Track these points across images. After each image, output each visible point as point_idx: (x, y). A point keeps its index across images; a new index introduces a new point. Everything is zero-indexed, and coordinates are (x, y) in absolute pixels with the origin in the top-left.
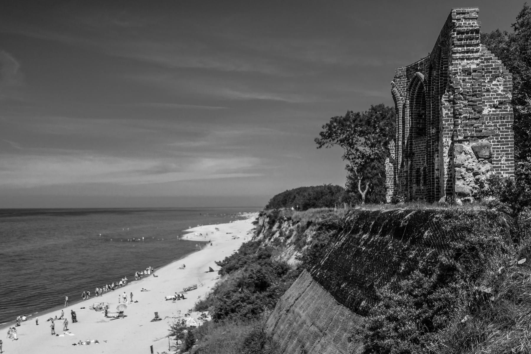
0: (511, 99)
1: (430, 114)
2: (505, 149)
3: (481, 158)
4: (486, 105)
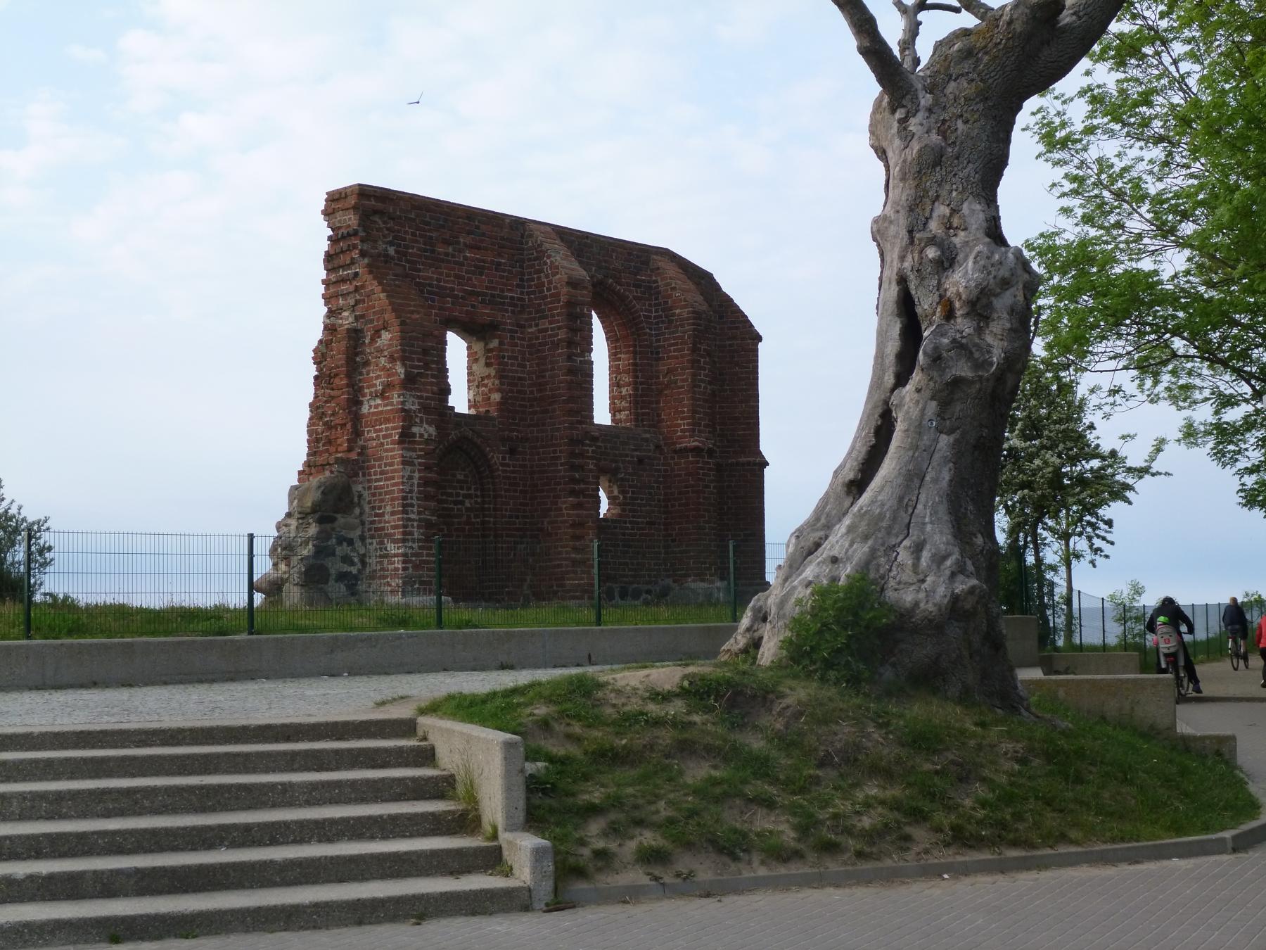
0: (402, 376)
2: (390, 489)
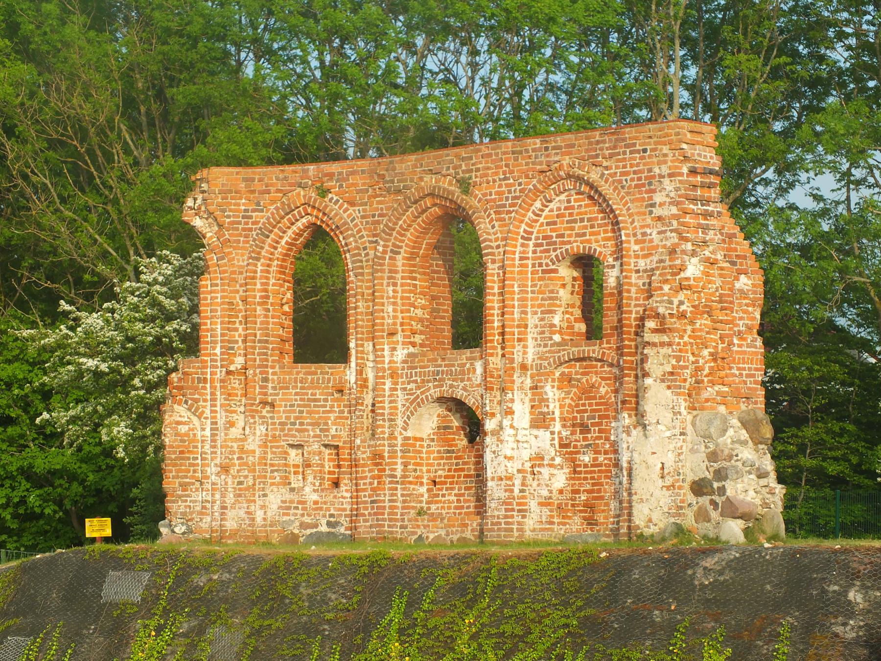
3: (761, 443)
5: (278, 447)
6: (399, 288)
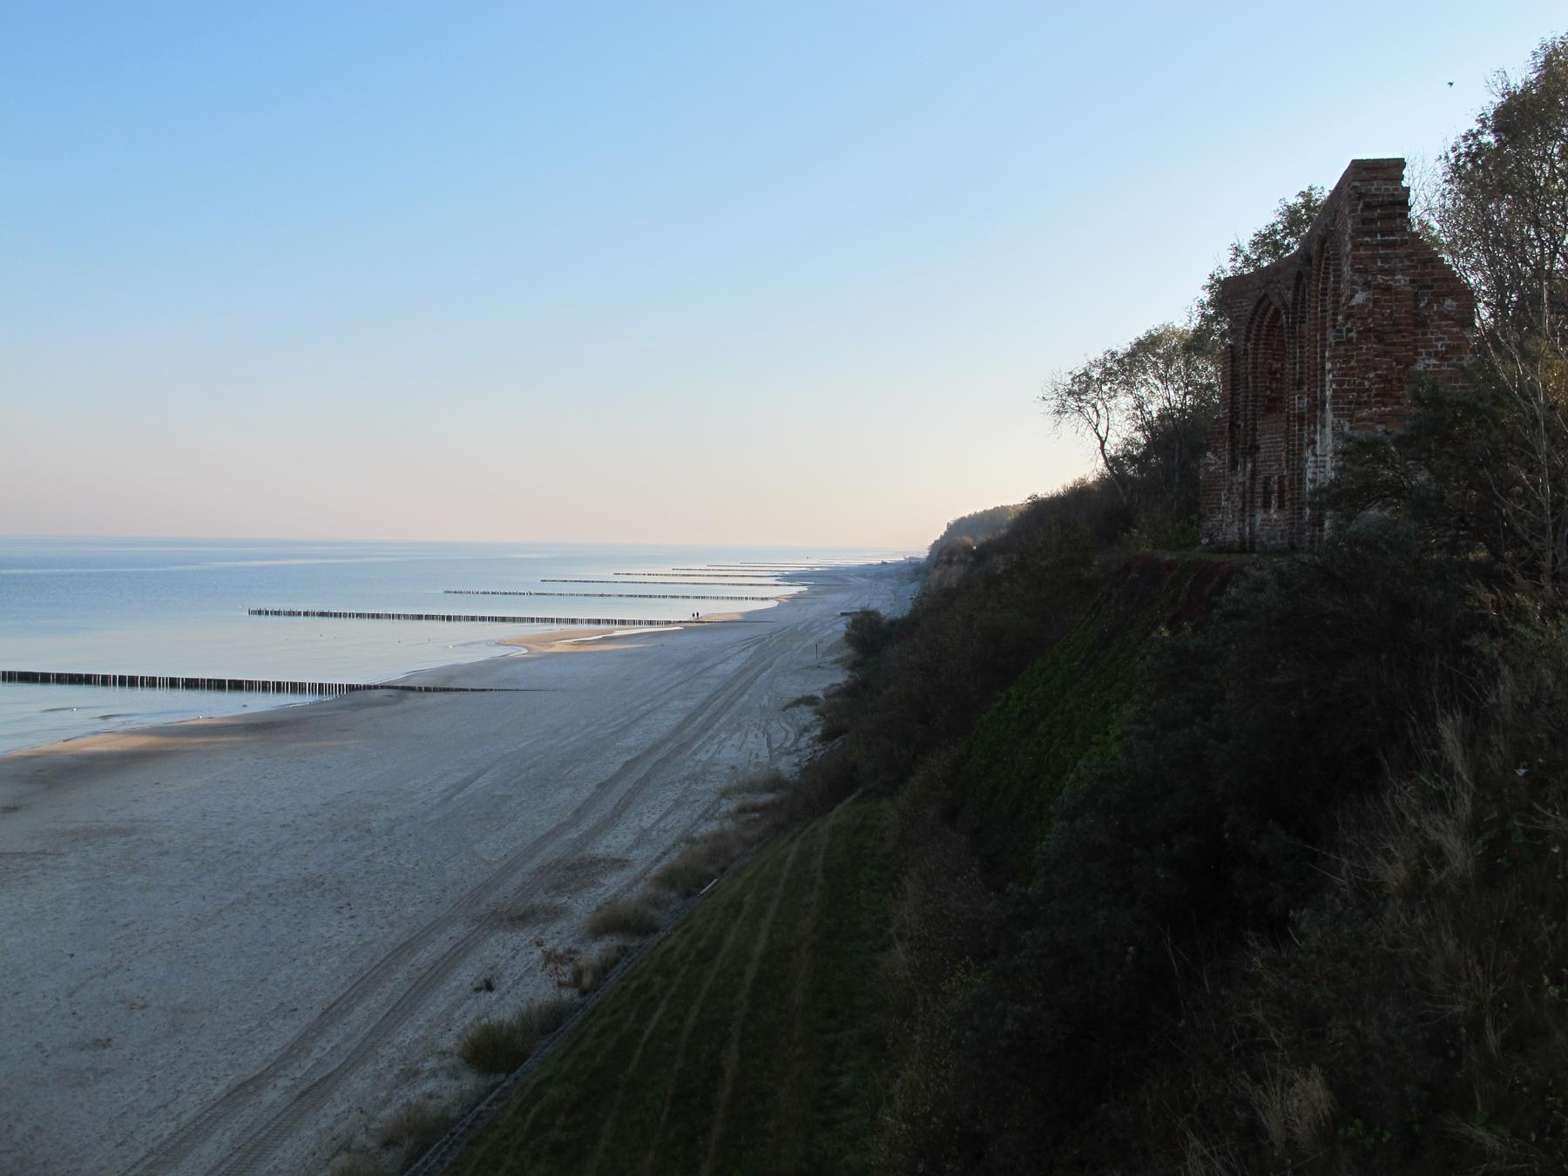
1: (1294, 369)
4: (1421, 354)
5: (1260, 479)
6: (1305, 350)
